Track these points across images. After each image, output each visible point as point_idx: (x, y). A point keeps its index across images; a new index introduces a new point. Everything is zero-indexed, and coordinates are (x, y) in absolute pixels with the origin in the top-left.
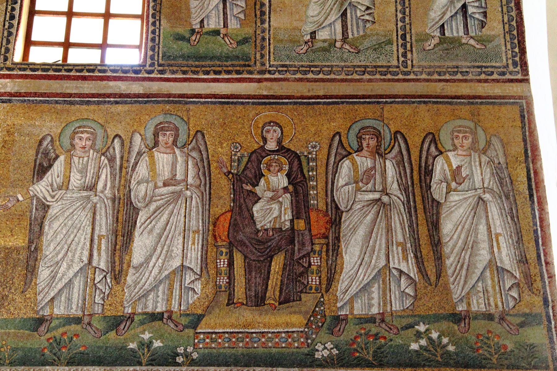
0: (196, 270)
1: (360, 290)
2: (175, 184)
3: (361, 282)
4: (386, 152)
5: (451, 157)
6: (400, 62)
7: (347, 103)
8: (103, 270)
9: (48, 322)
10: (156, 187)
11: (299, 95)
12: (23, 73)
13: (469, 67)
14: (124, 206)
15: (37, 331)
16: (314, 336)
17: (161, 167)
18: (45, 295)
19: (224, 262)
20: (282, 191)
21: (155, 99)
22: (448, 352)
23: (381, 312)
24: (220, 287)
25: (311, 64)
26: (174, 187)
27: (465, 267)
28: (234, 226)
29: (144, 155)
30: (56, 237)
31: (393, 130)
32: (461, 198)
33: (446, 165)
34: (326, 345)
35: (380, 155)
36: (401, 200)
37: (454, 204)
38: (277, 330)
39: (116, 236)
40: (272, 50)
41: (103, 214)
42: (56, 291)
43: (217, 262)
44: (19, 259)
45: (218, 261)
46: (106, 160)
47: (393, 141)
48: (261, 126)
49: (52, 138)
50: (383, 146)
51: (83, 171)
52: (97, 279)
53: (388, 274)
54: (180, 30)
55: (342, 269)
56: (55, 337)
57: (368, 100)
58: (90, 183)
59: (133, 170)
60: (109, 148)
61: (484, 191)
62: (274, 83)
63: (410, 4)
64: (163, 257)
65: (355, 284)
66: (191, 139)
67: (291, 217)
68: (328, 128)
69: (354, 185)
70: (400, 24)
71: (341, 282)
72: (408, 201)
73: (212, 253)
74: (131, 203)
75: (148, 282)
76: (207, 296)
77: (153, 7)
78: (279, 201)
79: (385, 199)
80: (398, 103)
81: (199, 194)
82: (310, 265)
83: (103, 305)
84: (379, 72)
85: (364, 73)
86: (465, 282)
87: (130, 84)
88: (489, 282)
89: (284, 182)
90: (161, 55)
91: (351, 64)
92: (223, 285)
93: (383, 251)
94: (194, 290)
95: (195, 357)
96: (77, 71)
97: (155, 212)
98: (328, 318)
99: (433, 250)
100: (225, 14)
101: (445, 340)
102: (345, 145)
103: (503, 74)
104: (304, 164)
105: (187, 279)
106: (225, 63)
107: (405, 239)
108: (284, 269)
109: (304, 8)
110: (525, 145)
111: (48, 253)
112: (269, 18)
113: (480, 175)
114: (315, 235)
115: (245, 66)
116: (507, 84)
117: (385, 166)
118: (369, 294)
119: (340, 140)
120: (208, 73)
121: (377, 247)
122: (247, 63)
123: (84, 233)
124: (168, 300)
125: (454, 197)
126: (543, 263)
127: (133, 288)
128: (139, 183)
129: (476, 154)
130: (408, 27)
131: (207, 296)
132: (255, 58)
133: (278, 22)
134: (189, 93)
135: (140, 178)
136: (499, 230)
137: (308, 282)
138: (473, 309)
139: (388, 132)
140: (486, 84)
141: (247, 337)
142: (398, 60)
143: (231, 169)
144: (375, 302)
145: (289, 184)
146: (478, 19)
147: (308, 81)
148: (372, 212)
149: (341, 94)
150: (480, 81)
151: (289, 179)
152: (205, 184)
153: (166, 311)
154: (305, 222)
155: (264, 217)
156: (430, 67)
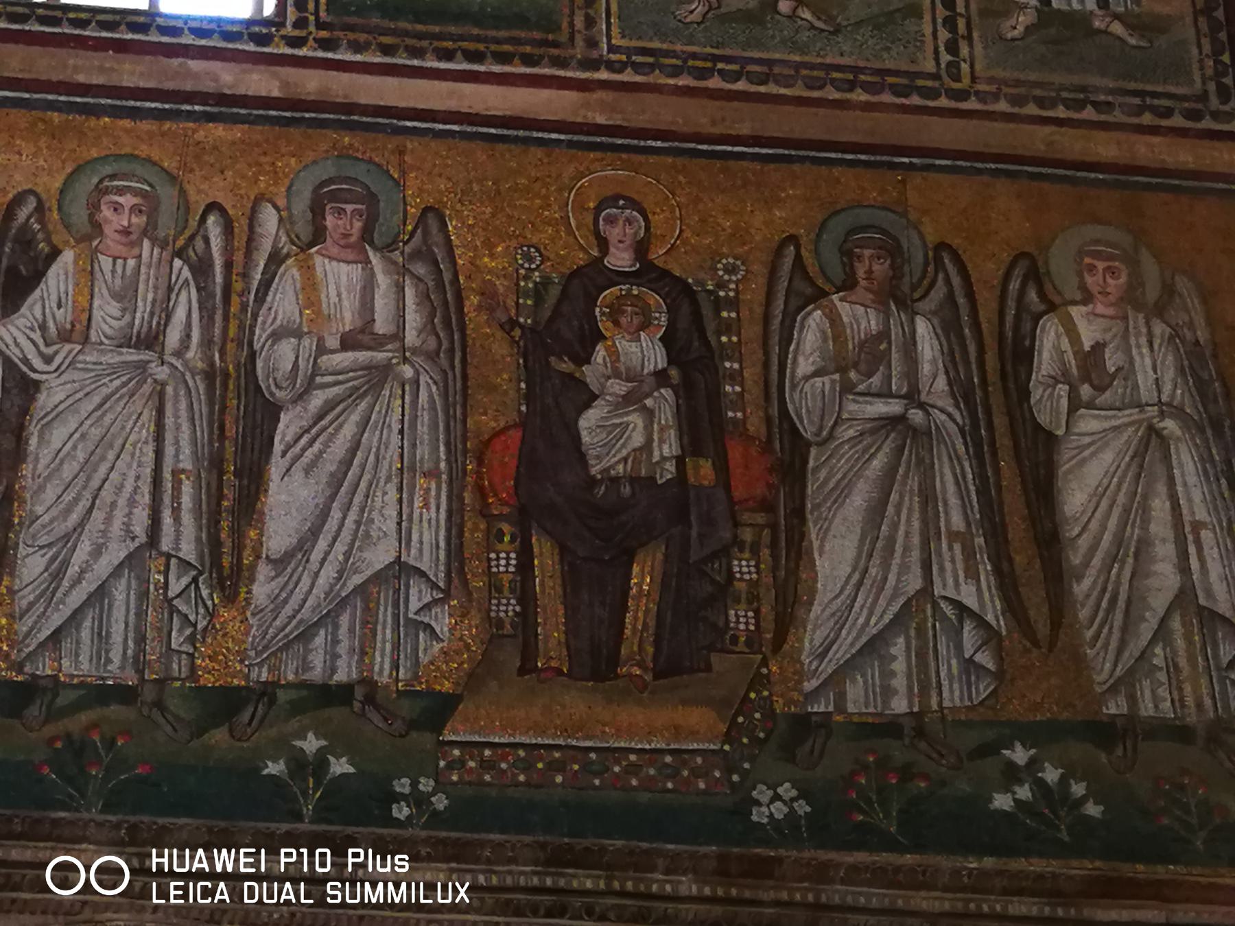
0: (436, 575)
1: (860, 651)
2: (372, 344)
4: (916, 295)
6: (943, 66)
8: (189, 564)
9: (49, 696)
10: (322, 350)
13: (1111, 92)
14: (239, 398)
16: (747, 766)
18: (36, 623)
19: (508, 559)
20: (651, 381)
21: (313, 115)
23: (916, 709)
24: (500, 623)
25: (715, 51)
26: (369, 354)
27: (1121, 603)
29: (290, 261)
30: (58, 469)
31: (931, 239)
32: (1107, 425)
34: (780, 790)
35: (902, 304)
36: (957, 424)
37: (1087, 440)
38: (653, 746)
39: (221, 473)
41: (183, 413)
43: (489, 560)
45: (493, 556)
46: (186, 268)
47: (931, 268)
48: (592, 205)
49: (40, 202)
50: (907, 279)
51: (126, 295)
52: (175, 587)
53: (929, 612)
55: (813, 592)
56: (68, 736)
57: (863, 157)
58: (145, 329)
60: (192, 238)
64: (346, 535)
65: (849, 633)
66: (410, 228)
67: (676, 451)
68: (766, 223)
69: (837, 376)
71: (809, 627)
75: (308, 604)
79: (916, 416)
84: (891, 86)
85: (852, 86)
87: (244, 71)
88: (1180, 643)
91: (819, 60)
92: (507, 621)
93: (916, 555)
94: (433, 630)
95: (441, 807)
97: (320, 417)
99: (1041, 557)
101: (1078, 789)
102: (810, 269)
104: (707, 311)
106: (492, 33)
107: (968, 524)
108: (665, 585)
111: (39, 510)
113: (1153, 369)
114: (740, 502)
115: (545, 43)
117: (914, 332)
119: (798, 256)
120: (448, 55)
122: (550, 37)
123: (135, 465)
124: (363, 653)
125: (1089, 423)
127: (270, 616)
128: (276, 336)
129: (1141, 316)
131: (467, 646)
132: (571, 24)
134: (403, 104)
135: (278, 322)
136: (1201, 515)
137: (727, 621)
138: (1143, 713)
139: (917, 241)
140: (1156, 140)
142: (937, 59)
143: (518, 315)
144: (899, 683)
145: (669, 363)
148: (886, 449)
152: (451, 350)
153: (362, 681)
154: (713, 463)
155: (609, 446)
156: (1018, 83)
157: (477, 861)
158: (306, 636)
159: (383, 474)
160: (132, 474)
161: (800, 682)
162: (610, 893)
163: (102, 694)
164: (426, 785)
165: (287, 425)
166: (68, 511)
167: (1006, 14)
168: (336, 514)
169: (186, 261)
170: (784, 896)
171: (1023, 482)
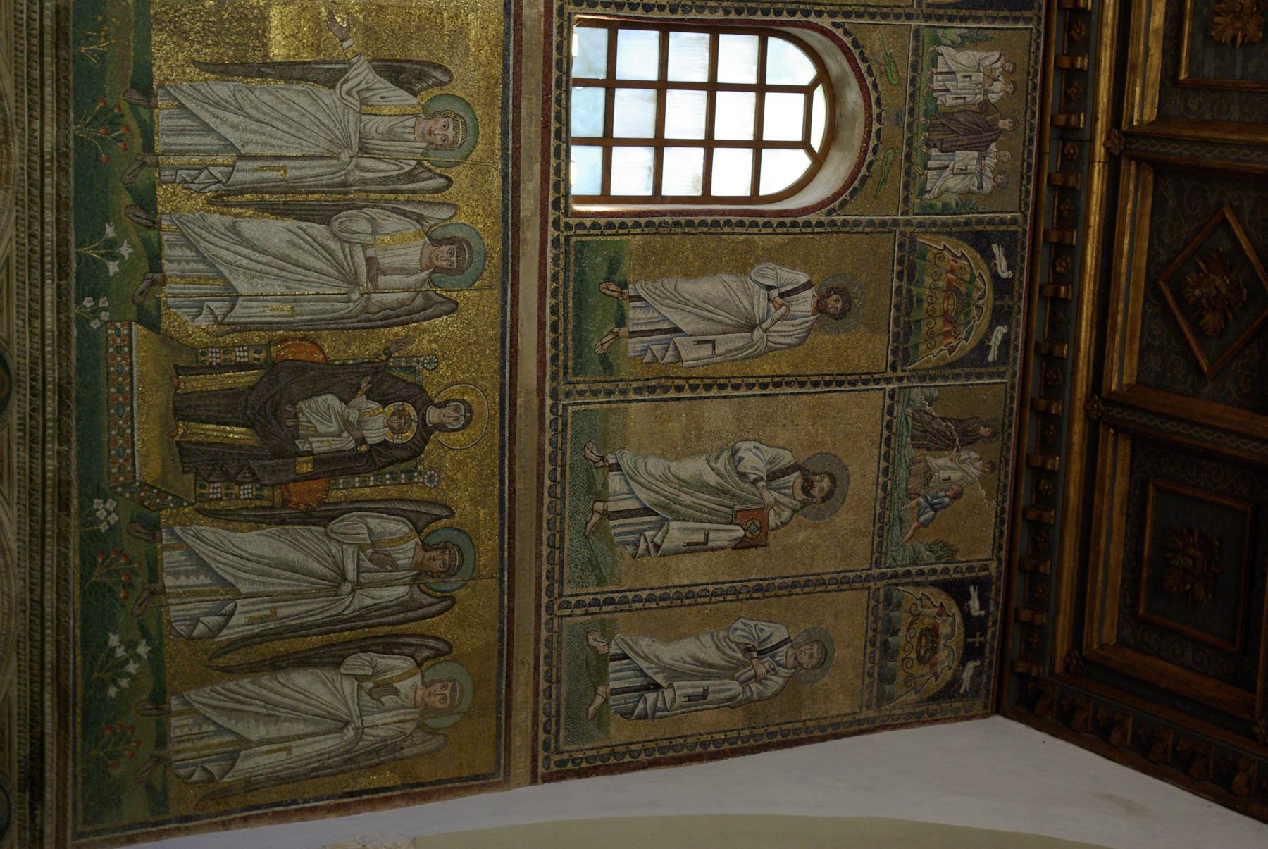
3: (214, 559)
5: (411, 681)
7: (502, 525)
10: (365, 246)
11: (517, 452)
12: (555, 30)
13: (558, 698)
15: (132, 87)
17: (397, 252)
20: (359, 435)
22: (105, 687)
27: (238, 706)
28: (300, 368)
29: (418, 226)
30: (283, 103)
32: (348, 696)
33: (400, 672)
35: (415, 581)
37: (338, 685)
39: (286, 193)
40: (592, 407)
42: (197, 110)
44: (246, 51)
51: (391, 135)
52: (214, 171)
54: (626, 265)
55: (235, 530)
56: (122, 116)
59: (394, 210)
61: (356, 729)
62: (536, 414)
63: (663, 608)
67: (316, 451)
68: (460, 498)
70: (631, 595)
71: (214, 529)
72: (341, 622)
73: (256, 337)
74: (340, 211)
76: (190, 336)
77: (665, 222)
78: (342, 432)
79: (346, 588)
80: (501, 599)
81: (353, 313)
82: (240, 484)
83: (174, 181)
86: (215, 708)
88: (216, 741)
89: (374, 437)
90: (584, 239)
93: (262, 589)
96: (558, 114)
97: (323, 247)
98: (153, 515)
100: (652, 332)
103: (546, 747)
104: (404, 466)
105: (216, 304)
106: (570, 337)
108: (232, 446)
109: (660, 452)
110: (431, 784)
111: (257, 93)
112: (644, 400)
113: (384, 723)
115: (566, 368)
116: (529, 753)
118: (193, 571)
119: (439, 518)
120: (554, 311)
121: (269, 580)
125: (348, 687)
126: (245, 814)
127: (200, 223)
128: (372, 221)
130: (626, 607)
131: (190, 336)
132: (578, 383)
133: (637, 413)
136: (296, 752)
140: (530, 724)
141: (125, 398)
142: (572, 596)
144: (183, 580)
145: (371, 446)
146: (636, 707)
147: (539, 464)
148: (325, 570)
149: (517, 514)
150: (535, 714)
151: (380, 444)
153: (164, 277)
155: (317, 412)
156: (559, 642)
157: (59, 346)
158: (189, 244)
159: (291, 284)
160: (282, 143)
161: (179, 524)
162: (45, 420)
163: (148, 134)
164: (105, 316)
165: (317, 229)
166: (257, 109)
167: (603, 635)
168: (264, 259)
169: (415, 168)
170: (49, 518)
171: (311, 650)
